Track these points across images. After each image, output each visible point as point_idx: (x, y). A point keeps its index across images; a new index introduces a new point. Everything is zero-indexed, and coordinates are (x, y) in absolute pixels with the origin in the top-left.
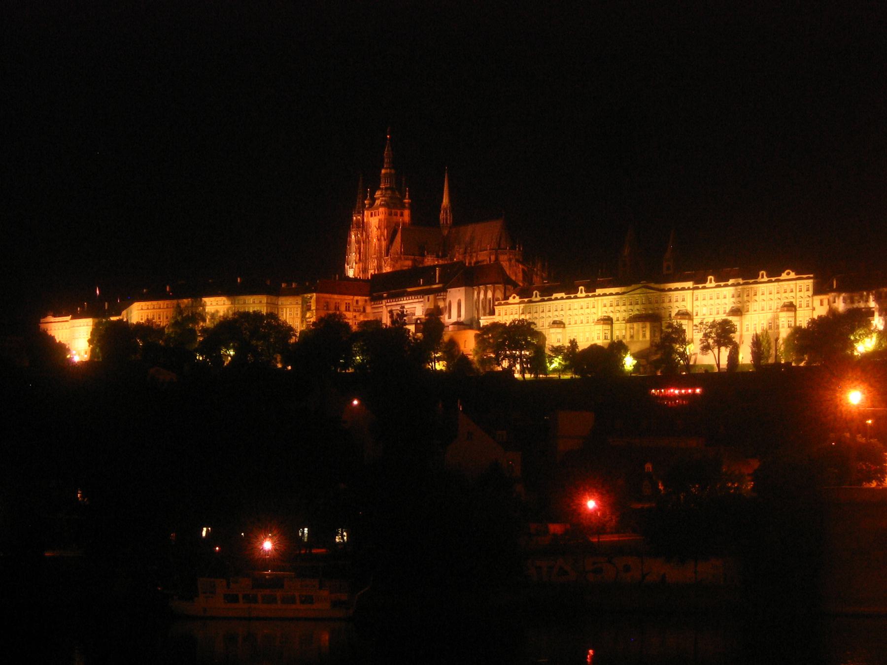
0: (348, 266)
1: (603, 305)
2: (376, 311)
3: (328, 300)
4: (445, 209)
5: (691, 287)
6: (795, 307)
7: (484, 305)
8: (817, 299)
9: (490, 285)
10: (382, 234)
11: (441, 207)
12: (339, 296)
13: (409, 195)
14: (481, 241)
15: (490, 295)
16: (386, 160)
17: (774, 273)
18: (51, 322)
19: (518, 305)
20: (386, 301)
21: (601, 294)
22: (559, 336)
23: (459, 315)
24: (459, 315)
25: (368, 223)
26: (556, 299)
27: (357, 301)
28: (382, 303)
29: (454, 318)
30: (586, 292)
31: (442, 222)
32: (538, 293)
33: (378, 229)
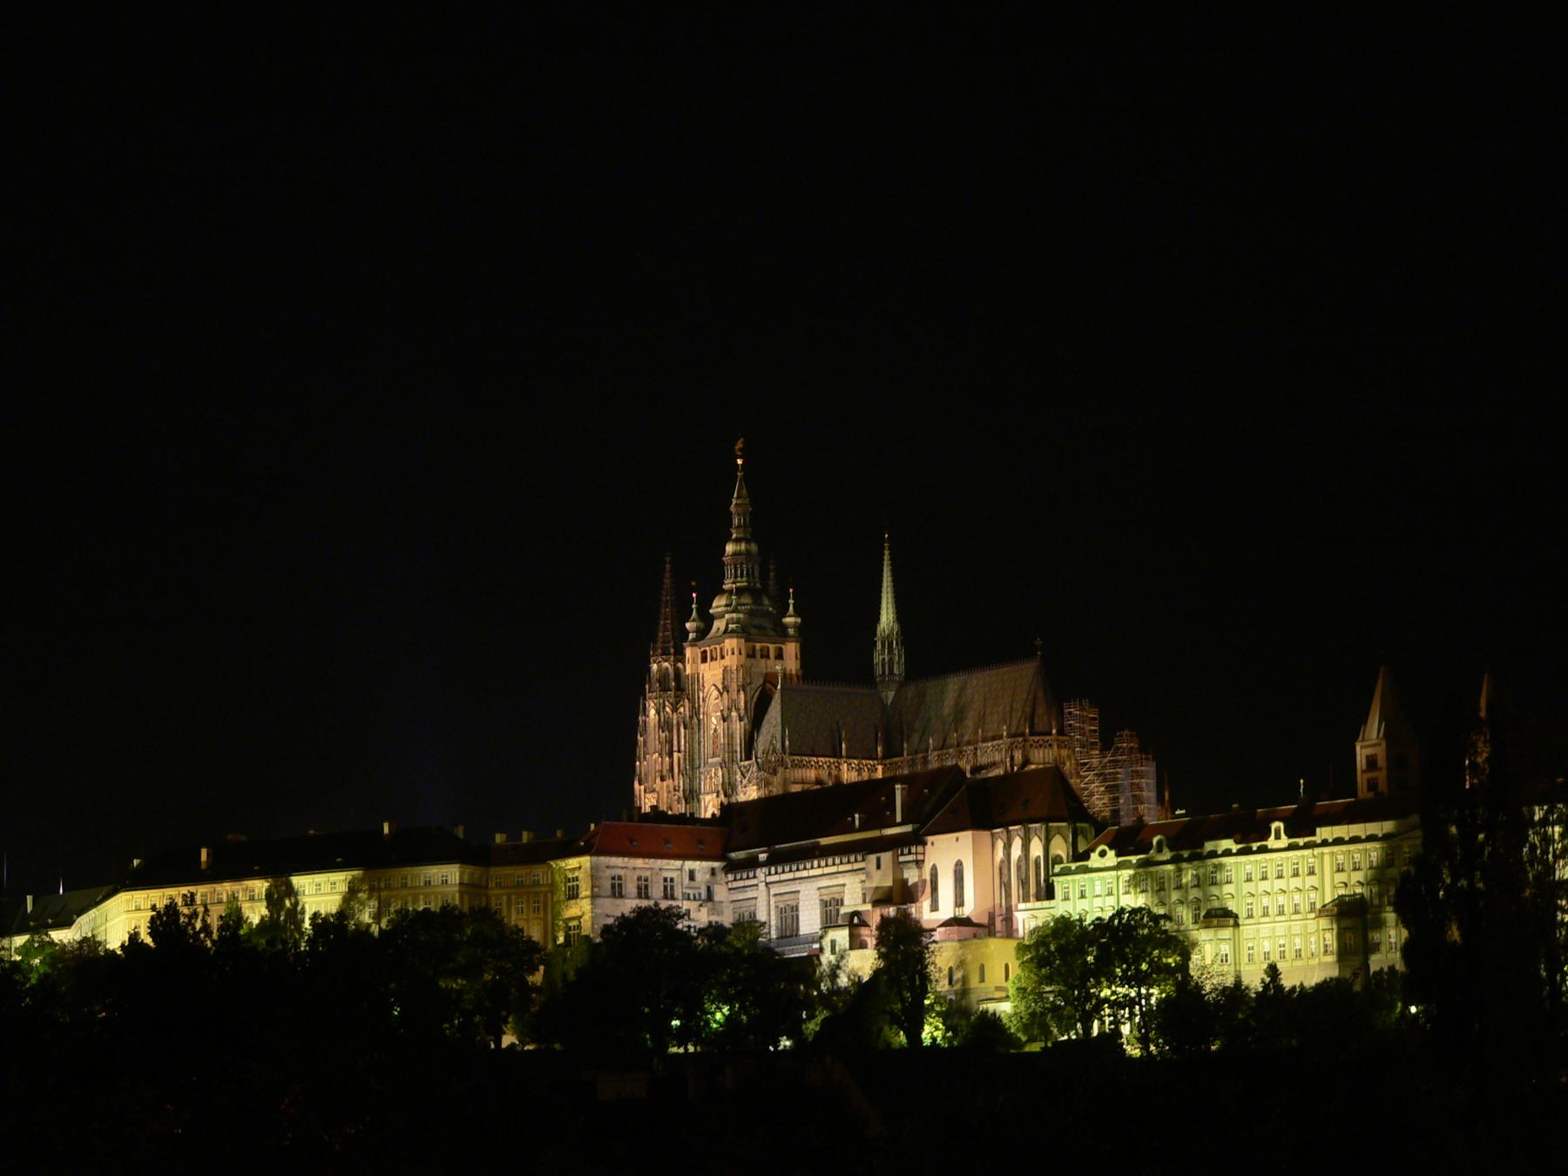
0: (642, 787)
2: (741, 897)
4: (887, 641)
7: (1023, 876)
11: (875, 635)
12: (647, 860)
13: (794, 604)
15: (1037, 849)
16: (736, 521)
19: (1113, 873)
20: (765, 870)
22: (1226, 948)
23: (959, 902)
24: (959, 902)
25: (696, 678)
29: (947, 910)
33: (721, 694)
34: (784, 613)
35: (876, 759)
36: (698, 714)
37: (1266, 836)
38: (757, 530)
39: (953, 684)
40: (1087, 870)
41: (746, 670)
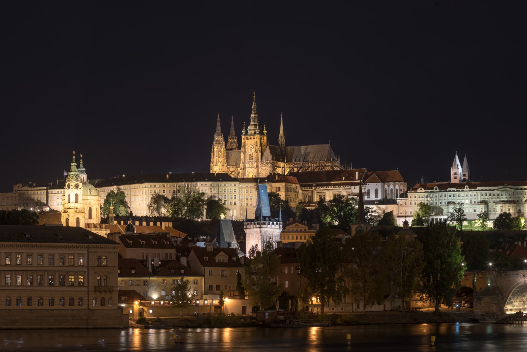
0: (213, 164)
1: (481, 195)
3: (288, 186)
9: (398, 182)
13: (265, 128)
15: (397, 187)
19: (425, 193)
21: (480, 190)
23: (377, 195)
24: (377, 195)
25: (244, 143)
26: (450, 191)
27: (296, 187)
30: (469, 188)
31: (280, 144)
34: (263, 130)
35: (284, 162)
36: (246, 150)
38: (257, 112)
39: (303, 148)
40: (417, 192)
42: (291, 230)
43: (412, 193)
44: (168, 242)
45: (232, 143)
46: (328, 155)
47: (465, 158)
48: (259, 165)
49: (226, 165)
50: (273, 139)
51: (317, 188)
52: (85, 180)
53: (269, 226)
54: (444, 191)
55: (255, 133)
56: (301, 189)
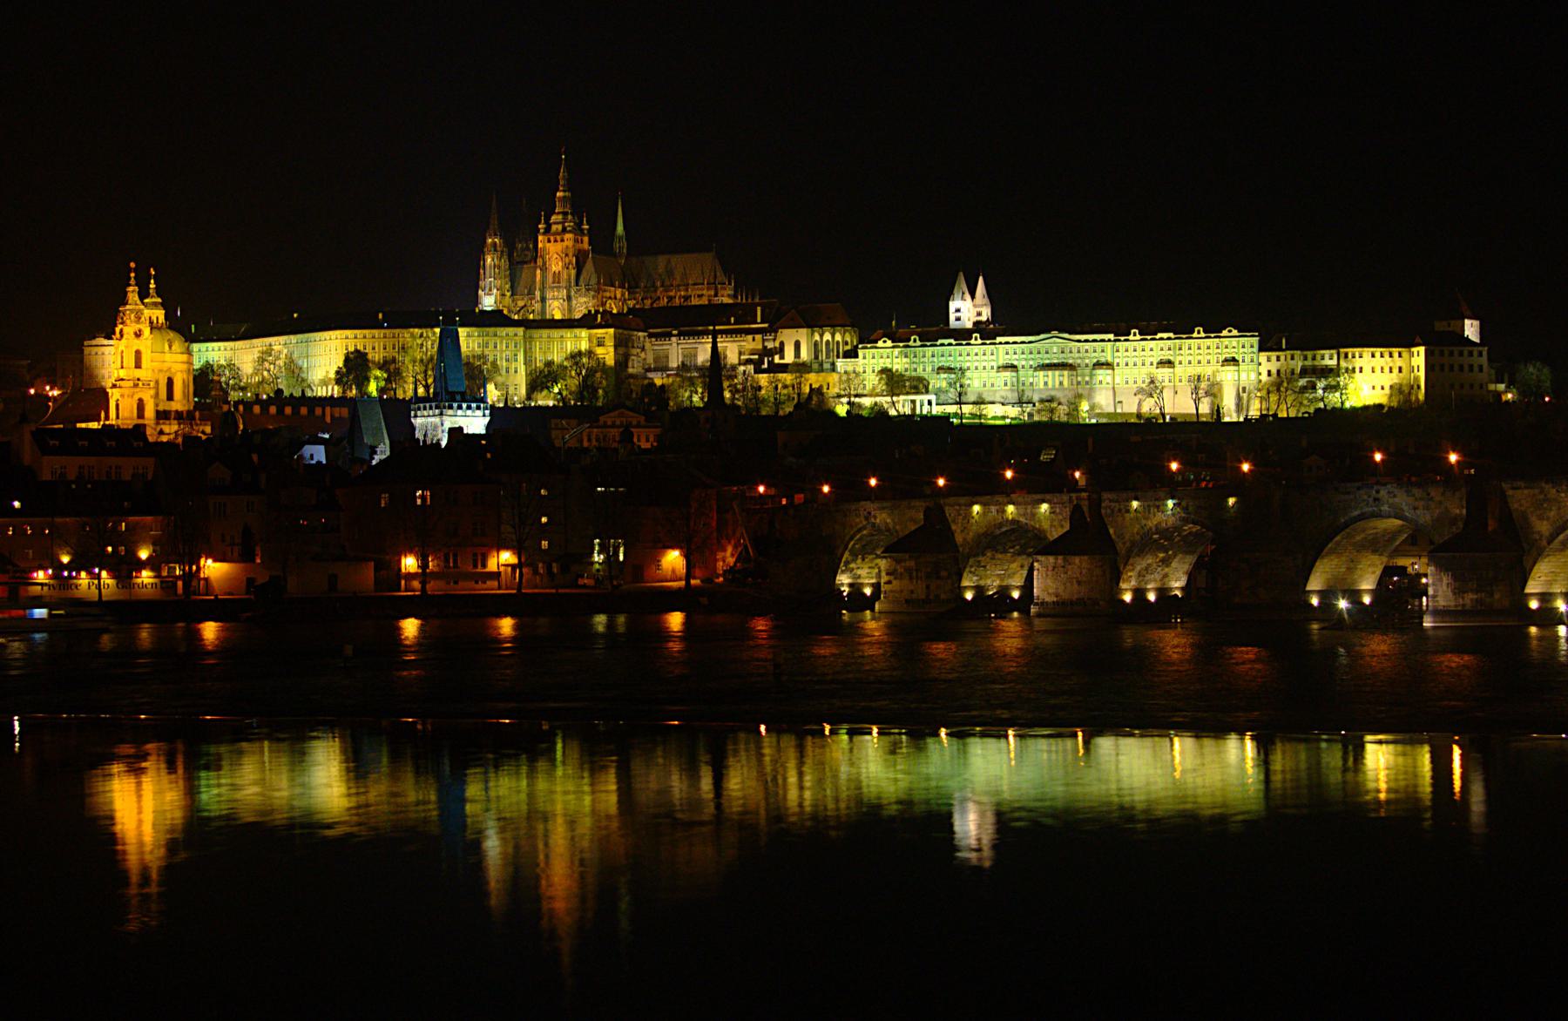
4: (620, 238)
5: (1112, 339)
6: (1238, 361)
8: (1263, 356)
10: (570, 263)
14: (686, 274)
15: (838, 337)
16: (561, 182)
17: (1213, 328)
18: (104, 346)
26: (942, 345)
28: (669, 340)
32: (917, 338)
34: (582, 224)
35: (624, 288)
37: (971, 339)
39: (661, 261)
40: (876, 348)
41: (574, 246)
42: (609, 423)
43: (866, 348)
44: (141, 444)
45: (523, 250)
46: (710, 272)
47: (981, 279)
48: (573, 293)
49: (508, 294)
50: (601, 241)
51: (680, 339)
52: (160, 322)
53: (460, 412)
54: (931, 346)
55: (564, 230)
56: (651, 342)
